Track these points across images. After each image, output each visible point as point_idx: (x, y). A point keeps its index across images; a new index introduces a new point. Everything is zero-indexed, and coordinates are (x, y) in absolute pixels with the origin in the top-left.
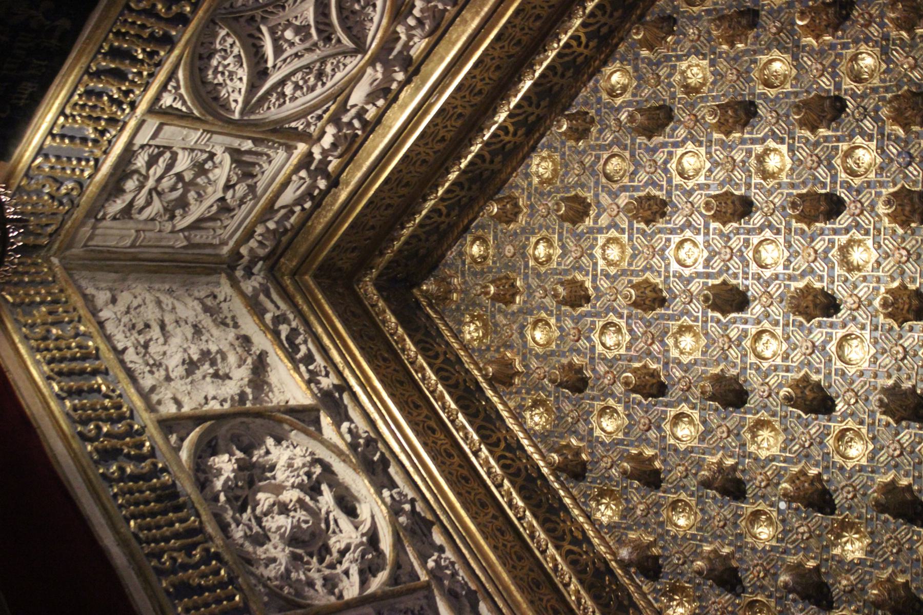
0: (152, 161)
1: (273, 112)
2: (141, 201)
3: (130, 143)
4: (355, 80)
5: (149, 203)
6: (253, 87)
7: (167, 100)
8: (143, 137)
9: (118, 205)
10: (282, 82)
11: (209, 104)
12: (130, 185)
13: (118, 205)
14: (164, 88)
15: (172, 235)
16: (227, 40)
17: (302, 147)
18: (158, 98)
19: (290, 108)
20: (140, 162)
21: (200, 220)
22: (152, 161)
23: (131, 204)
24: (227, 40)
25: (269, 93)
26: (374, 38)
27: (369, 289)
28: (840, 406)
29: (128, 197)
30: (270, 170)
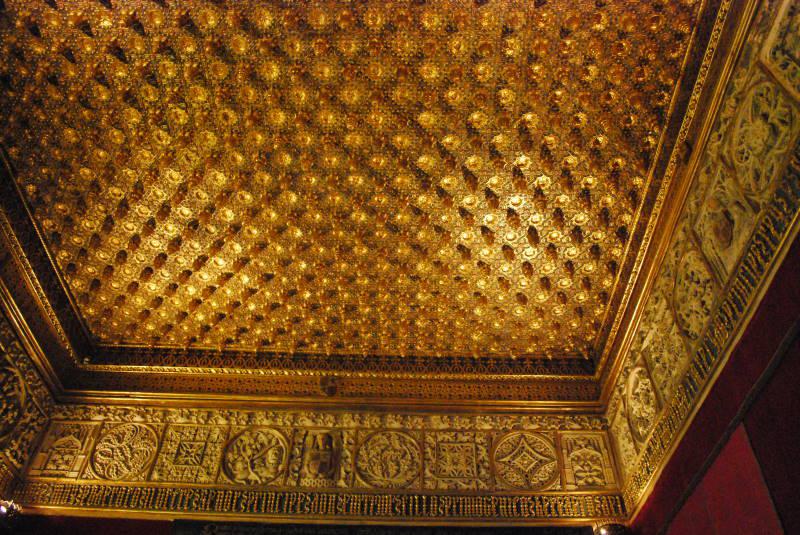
0: (580, 478)
1: (551, 450)
2: (595, 473)
3: (576, 490)
4: (531, 431)
5: (596, 470)
6: (546, 462)
7: (559, 487)
8: (573, 487)
9: (598, 480)
10: (541, 454)
11: (558, 473)
12: (590, 480)
13: (598, 480)
14: (555, 490)
15: (603, 456)
16: (535, 482)
17: (559, 432)
18: (560, 491)
19: (548, 445)
20: (581, 482)
21: (596, 449)
22: (580, 478)
23: (597, 476)
24: (535, 482)
25: (545, 456)
26: (515, 435)
27: (597, 376)
28: (522, 261)
29: (595, 478)
30: (570, 437)
